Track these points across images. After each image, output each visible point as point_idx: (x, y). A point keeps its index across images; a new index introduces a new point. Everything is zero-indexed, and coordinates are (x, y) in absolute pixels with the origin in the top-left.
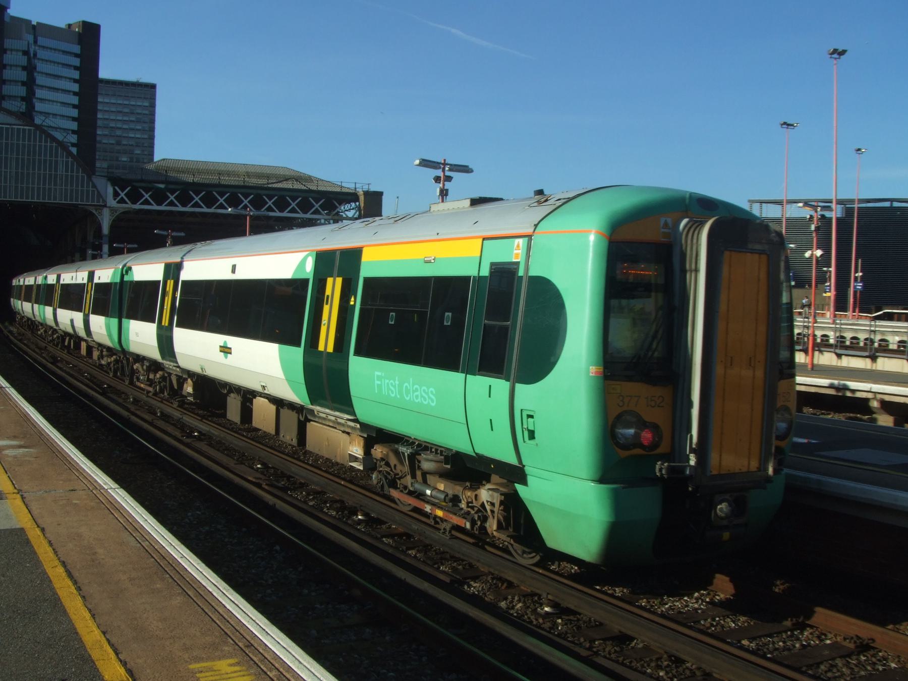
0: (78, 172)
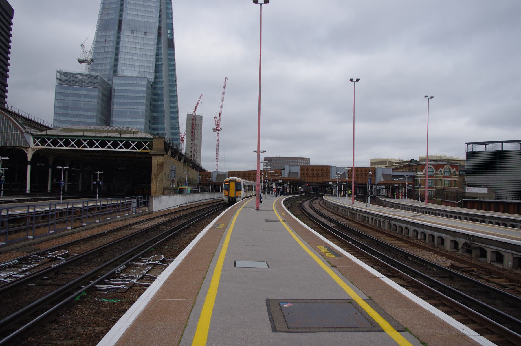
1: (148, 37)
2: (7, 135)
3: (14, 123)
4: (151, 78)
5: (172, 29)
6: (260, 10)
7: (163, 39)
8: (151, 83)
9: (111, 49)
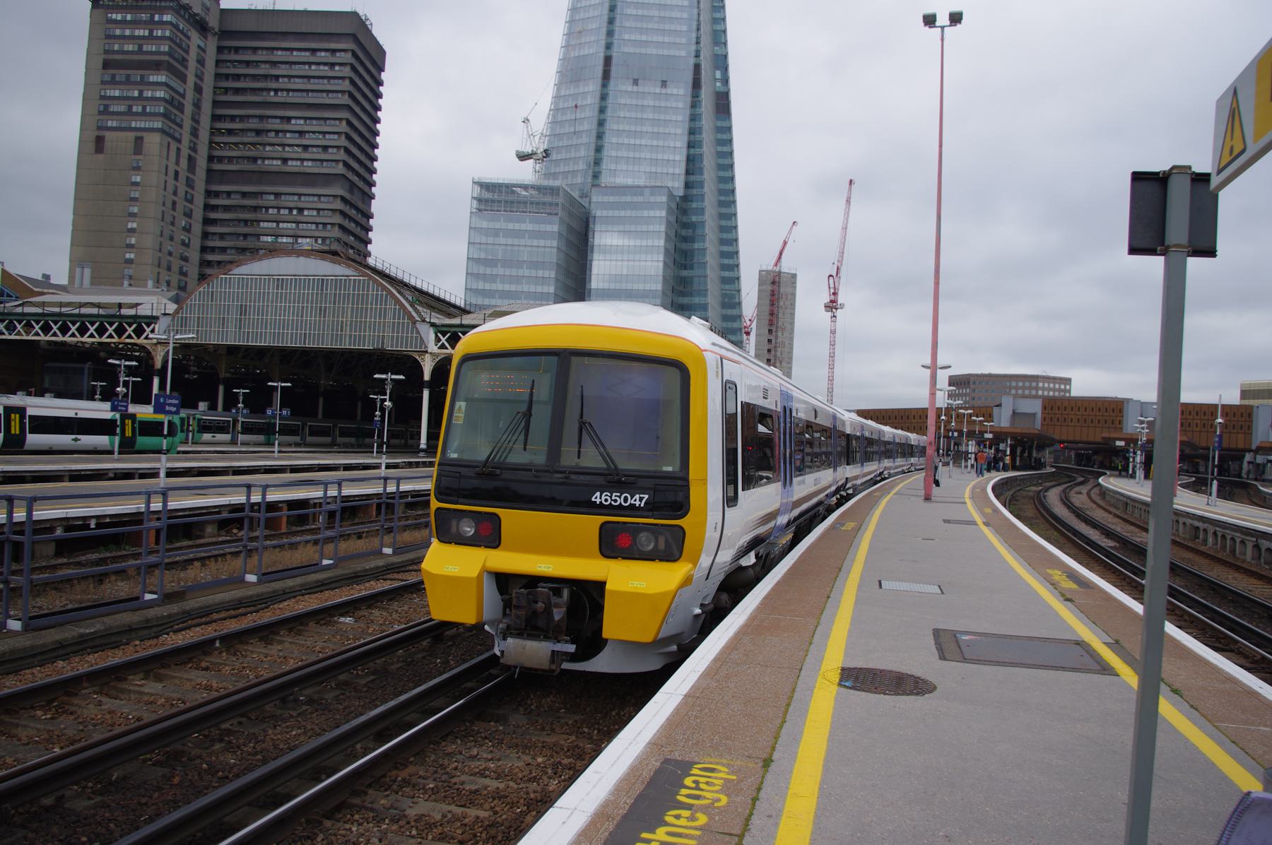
0: (404, 319)
1: (669, 91)
2: (384, 326)
3: (398, 301)
4: (678, 186)
5: (725, 69)
6: (940, 42)
7: (706, 95)
8: (678, 199)
9: (589, 126)
